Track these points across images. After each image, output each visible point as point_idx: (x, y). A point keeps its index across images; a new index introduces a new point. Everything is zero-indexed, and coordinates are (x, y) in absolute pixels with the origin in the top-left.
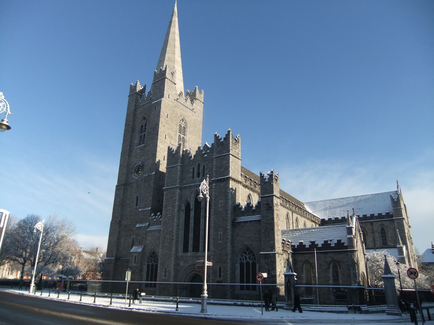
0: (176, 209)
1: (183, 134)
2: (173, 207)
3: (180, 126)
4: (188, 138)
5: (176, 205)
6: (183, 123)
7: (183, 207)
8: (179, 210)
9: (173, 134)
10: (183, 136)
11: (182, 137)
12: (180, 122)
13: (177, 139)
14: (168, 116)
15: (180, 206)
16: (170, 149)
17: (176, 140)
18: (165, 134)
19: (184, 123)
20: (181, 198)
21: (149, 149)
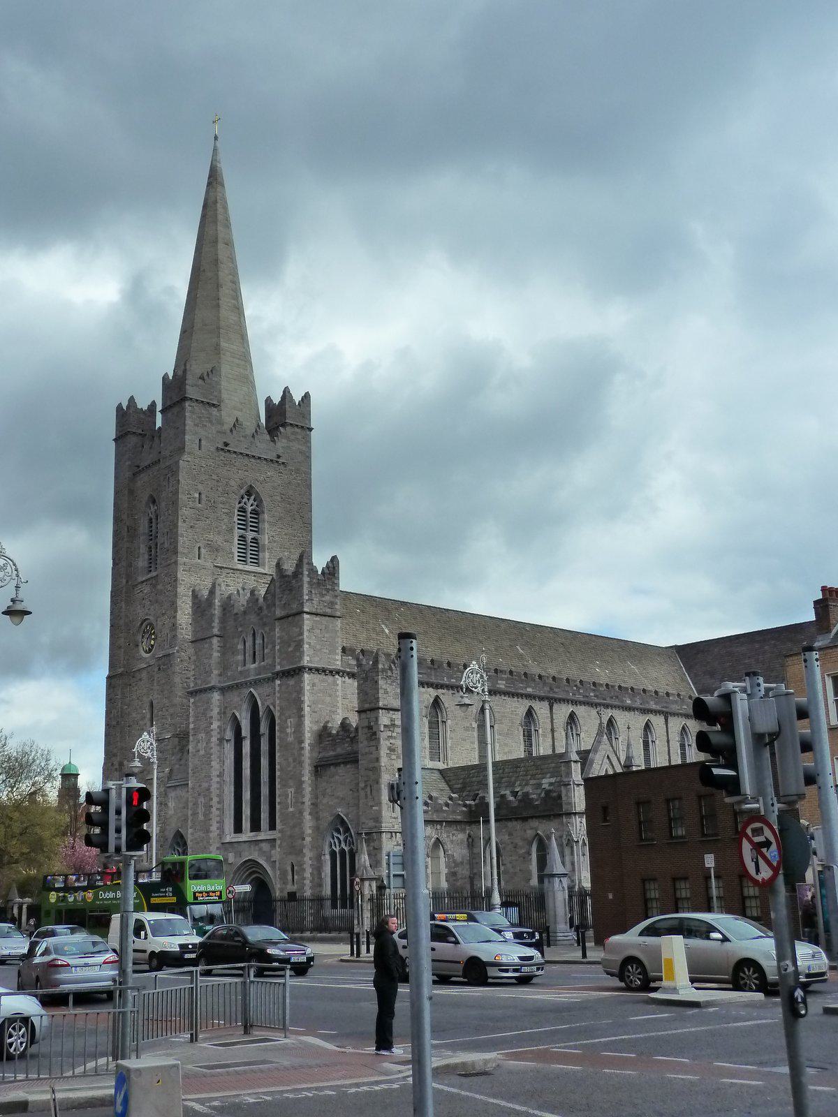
0: (214, 739)
1: (251, 530)
2: (208, 732)
3: (242, 510)
4: (269, 538)
5: (212, 730)
6: (251, 501)
7: (229, 734)
8: (221, 740)
9: (219, 540)
10: (253, 535)
11: (249, 539)
12: (240, 503)
13: (235, 550)
14: (203, 496)
15: (222, 730)
16: (195, 595)
17: (232, 553)
18: (198, 545)
19: (255, 500)
20: (225, 713)
21: (162, 588)
